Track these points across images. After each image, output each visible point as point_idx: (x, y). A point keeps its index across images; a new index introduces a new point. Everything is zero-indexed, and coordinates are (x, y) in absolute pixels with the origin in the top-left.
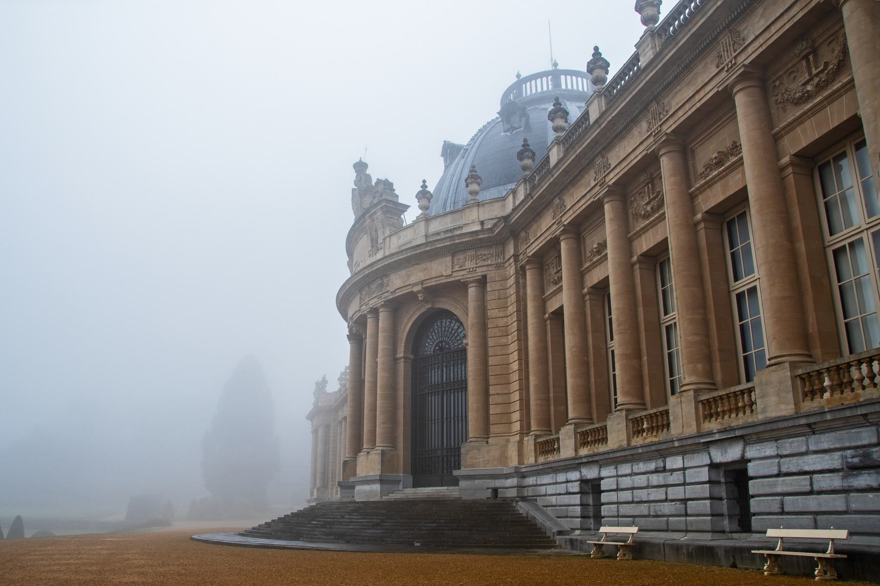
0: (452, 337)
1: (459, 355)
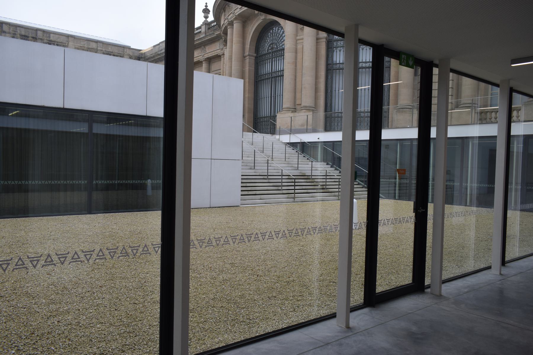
0: (279, 40)
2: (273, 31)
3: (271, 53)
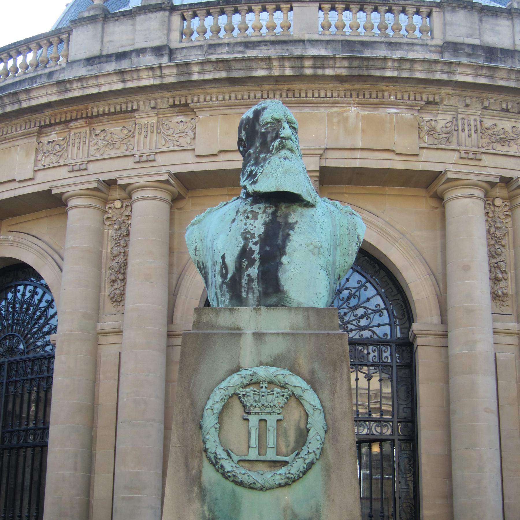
0: (33, 327)
2: (15, 296)
3: (6, 366)
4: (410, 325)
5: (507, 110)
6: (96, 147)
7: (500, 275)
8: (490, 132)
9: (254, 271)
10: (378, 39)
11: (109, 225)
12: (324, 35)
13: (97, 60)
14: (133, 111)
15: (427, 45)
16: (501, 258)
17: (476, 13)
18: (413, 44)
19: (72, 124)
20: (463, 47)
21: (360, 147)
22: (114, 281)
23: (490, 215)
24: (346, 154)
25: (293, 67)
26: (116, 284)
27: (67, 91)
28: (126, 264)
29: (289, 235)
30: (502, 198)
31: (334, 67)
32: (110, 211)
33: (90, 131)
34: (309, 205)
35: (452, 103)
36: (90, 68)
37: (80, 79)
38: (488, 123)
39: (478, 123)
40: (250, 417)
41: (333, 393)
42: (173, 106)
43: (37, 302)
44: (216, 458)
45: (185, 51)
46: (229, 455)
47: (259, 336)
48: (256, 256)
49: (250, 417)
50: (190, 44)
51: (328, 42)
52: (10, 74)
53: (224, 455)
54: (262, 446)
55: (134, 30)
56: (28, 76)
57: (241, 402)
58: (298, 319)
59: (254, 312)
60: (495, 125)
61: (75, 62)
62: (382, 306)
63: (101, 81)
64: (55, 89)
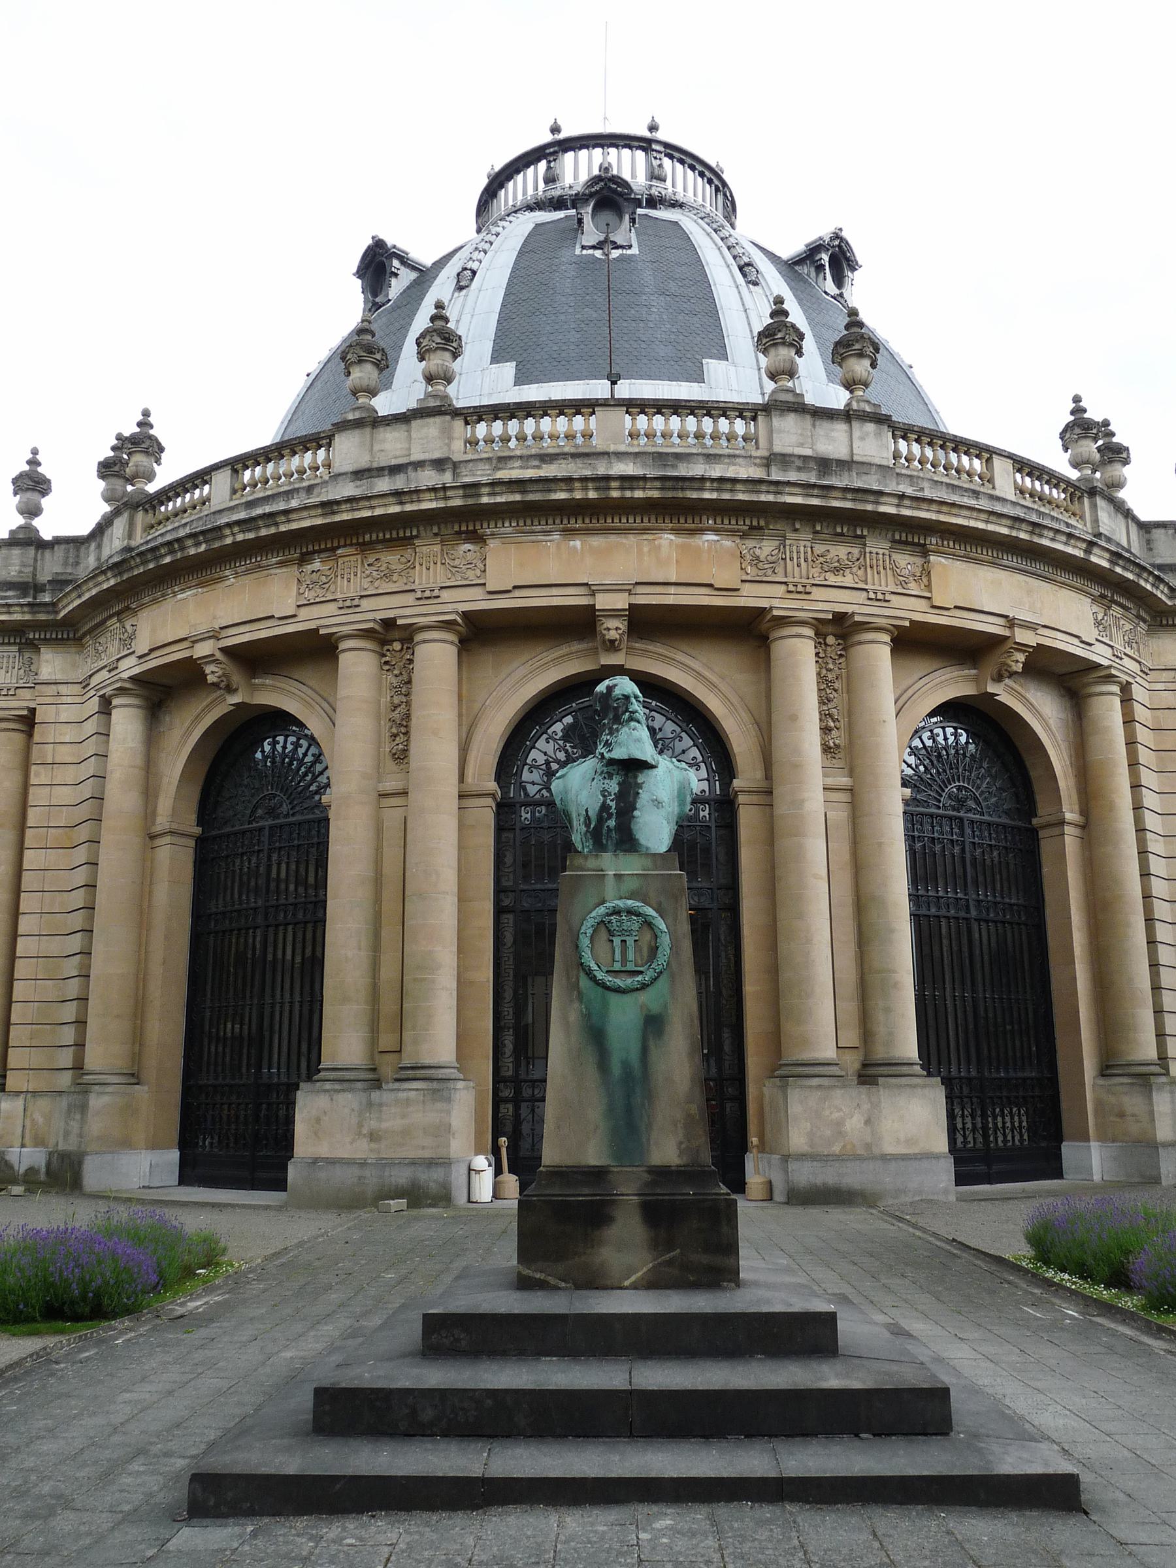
1: (314, 832)
3: (266, 832)
4: (731, 781)
5: (842, 534)
6: (369, 579)
7: (832, 724)
8: (821, 559)
9: (612, 823)
10: (694, 451)
11: (388, 670)
12: (632, 445)
13: (366, 474)
14: (412, 538)
15: (751, 457)
16: (832, 703)
17: (808, 417)
18: (734, 456)
19: (339, 551)
20: (793, 459)
21: (673, 581)
22: (395, 736)
23: (820, 655)
24: (658, 589)
25: (597, 489)
26: (398, 739)
27: (333, 513)
28: (408, 717)
29: (638, 793)
30: (835, 635)
31: (644, 489)
32: (388, 653)
33: (362, 561)
34: (653, 767)
35: (778, 527)
36: (359, 483)
37: (351, 500)
38: (819, 549)
39: (809, 549)
40: (614, 939)
41: (675, 919)
42: (460, 533)
43: (301, 756)
44: (590, 970)
45: (471, 464)
46: (599, 967)
47: (618, 877)
48: (613, 810)
49: (614, 939)
50: (476, 457)
51: (637, 455)
52: (259, 485)
53: (596, 968)
54: (624, 961)
55: (409, 438)
56: (282, 489)
57: (607, 927)
58: (648, 862)
59: (613, 857)
60: (828, 551)
61: (340, 475)
62: (700, 758)
63: (375, 502)
64: (319, 511)
